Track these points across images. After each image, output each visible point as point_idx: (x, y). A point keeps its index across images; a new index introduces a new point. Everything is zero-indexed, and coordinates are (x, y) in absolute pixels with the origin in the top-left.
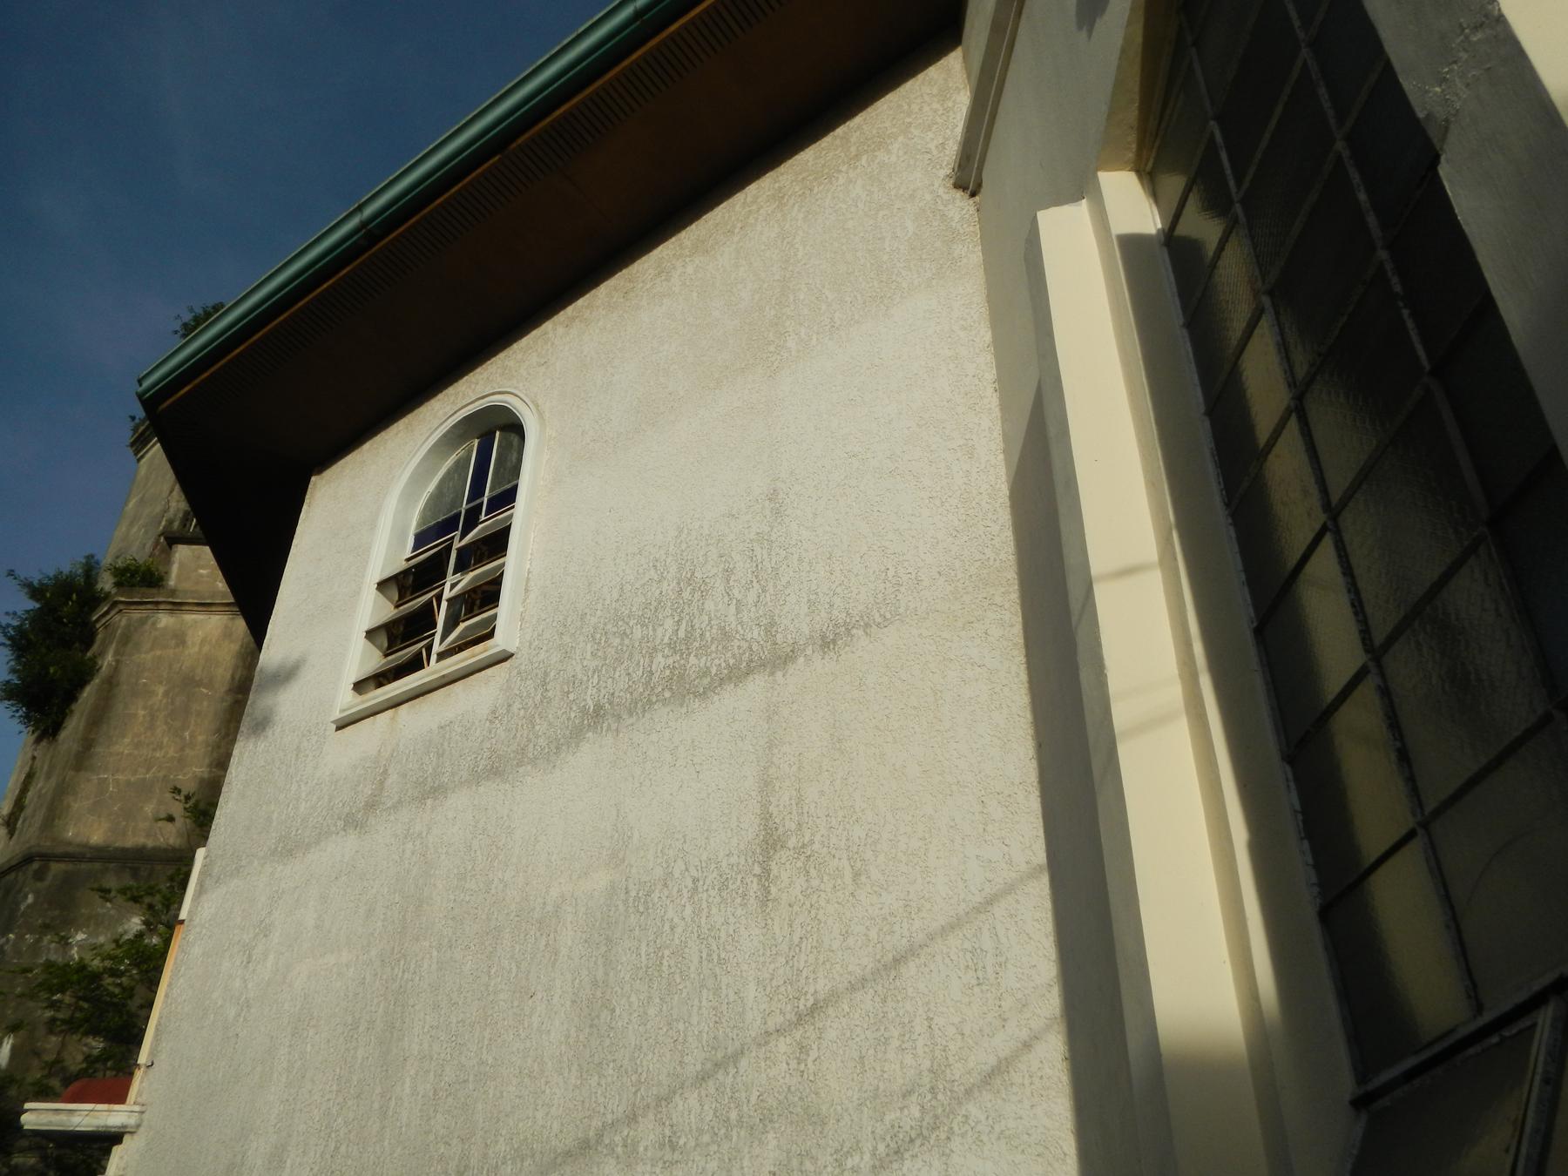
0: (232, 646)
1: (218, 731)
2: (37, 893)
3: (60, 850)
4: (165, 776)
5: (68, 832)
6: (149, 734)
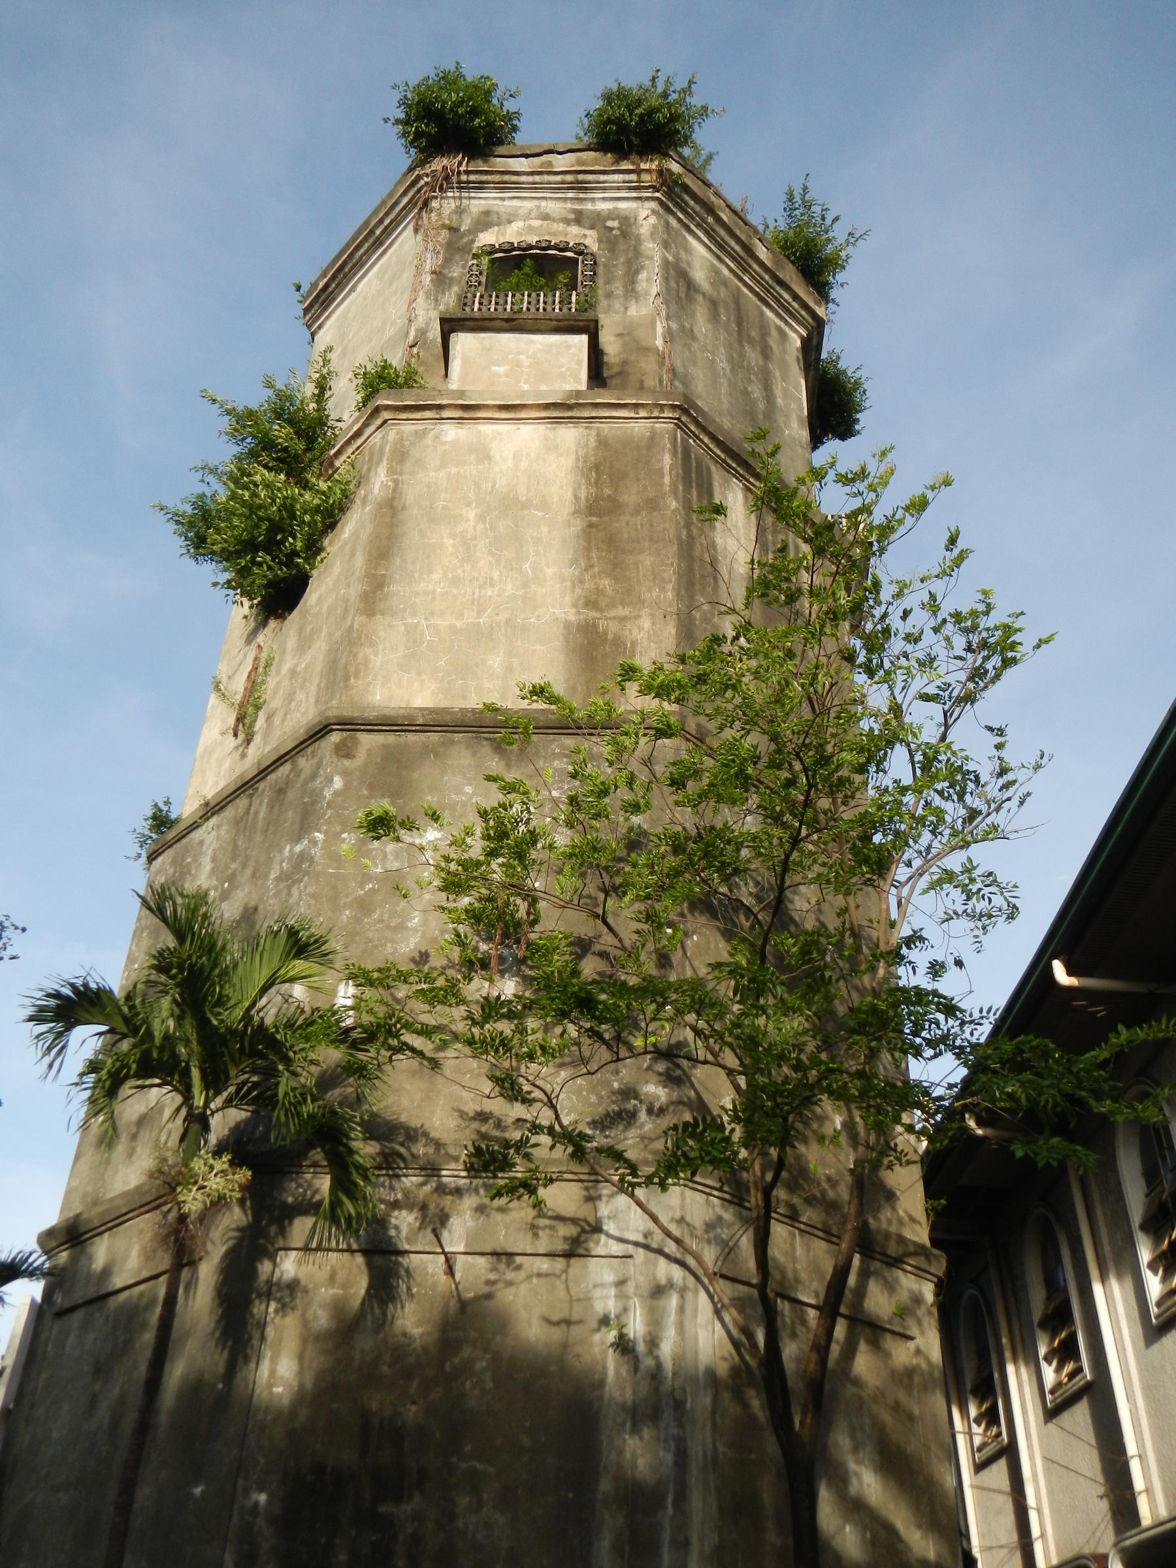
0: (563, 460)
1: (574, 562)
2: (345, 774)
3: (371, 715)
4: (508, 621)
5: (375, 694)
6: (468, 567)
